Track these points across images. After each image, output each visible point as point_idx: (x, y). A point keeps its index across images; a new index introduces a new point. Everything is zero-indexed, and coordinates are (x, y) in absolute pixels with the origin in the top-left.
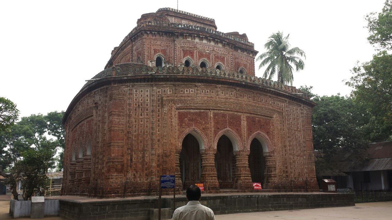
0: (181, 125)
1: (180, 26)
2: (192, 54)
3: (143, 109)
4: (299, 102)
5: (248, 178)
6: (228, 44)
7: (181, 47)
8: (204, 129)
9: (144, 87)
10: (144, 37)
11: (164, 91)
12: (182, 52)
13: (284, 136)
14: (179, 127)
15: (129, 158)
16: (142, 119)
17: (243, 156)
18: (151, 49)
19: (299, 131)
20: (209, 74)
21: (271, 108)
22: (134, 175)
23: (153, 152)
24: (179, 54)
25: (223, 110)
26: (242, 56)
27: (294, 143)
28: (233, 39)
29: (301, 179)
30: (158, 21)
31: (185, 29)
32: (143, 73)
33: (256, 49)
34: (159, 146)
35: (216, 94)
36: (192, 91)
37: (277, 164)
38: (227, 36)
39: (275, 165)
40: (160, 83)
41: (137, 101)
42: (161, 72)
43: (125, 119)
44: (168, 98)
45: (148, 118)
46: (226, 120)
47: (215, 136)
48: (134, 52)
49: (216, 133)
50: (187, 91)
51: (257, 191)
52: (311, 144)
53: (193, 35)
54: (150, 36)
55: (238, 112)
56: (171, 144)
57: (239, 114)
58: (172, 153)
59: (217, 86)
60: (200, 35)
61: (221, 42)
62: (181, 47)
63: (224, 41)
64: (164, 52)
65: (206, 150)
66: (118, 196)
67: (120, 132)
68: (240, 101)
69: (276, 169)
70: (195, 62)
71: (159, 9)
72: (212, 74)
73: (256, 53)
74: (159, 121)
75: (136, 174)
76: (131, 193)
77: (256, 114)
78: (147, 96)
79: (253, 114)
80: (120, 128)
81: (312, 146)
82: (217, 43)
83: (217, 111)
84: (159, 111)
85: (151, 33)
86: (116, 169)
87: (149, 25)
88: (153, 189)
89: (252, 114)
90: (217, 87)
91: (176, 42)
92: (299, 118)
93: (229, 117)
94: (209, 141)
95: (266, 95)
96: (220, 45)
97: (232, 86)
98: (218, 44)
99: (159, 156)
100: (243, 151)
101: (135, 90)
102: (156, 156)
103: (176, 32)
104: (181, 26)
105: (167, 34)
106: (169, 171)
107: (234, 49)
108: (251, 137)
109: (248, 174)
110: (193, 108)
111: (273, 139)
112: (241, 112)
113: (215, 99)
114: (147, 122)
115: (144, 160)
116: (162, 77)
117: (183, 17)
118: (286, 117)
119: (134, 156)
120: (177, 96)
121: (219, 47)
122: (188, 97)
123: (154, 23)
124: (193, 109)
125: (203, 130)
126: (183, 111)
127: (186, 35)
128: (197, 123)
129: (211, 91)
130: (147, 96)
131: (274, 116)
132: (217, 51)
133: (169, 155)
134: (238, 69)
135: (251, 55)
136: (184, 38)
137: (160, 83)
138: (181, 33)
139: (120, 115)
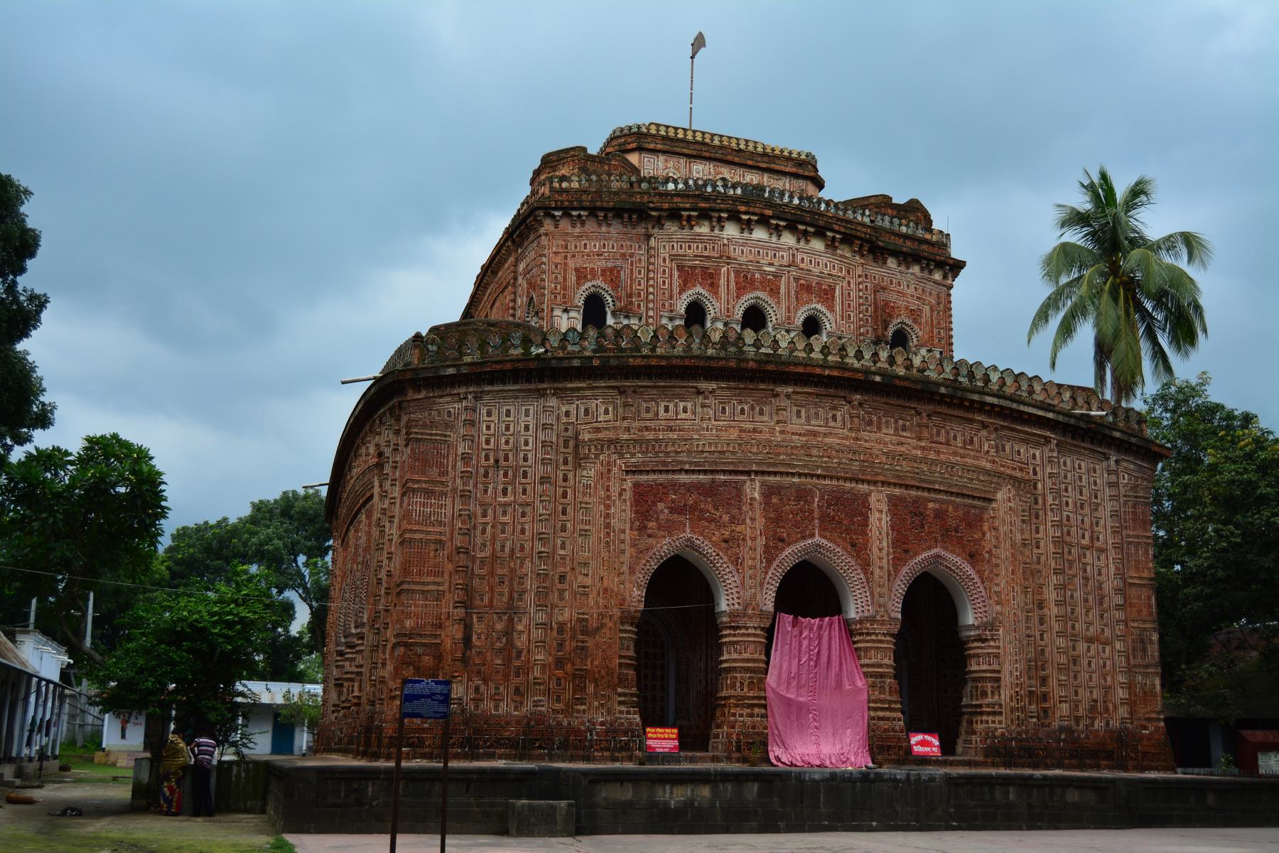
0: (642, 528)
1: (671, 186)
2: (710, 279)
3: (510, 473)
4: (1100, 446)
5: (888, 714)
6: (847, 240)
7: (673, 258)
8: (726, 541)
9: (517, 397)
10: (542, 231)
11: (587, 411)
12: (676, 273)
14: (636, 533)
15: (460, 635)
16: (506, 505)
17: (873, 637)
18: (565, 270)
19: (1101, 550)
20: (752, 349)
21: (988, 466)
22: (477, 689)
23: (541, 617)
25: (800, 475)
26: (904, 282)
28: (867, 220)
29: (1098, 724)
30: (595, 172)
31: (688, 196)
32: (512, 351)
33: (956, 253)
35: (776, 419)
37: (1007, 668)
38: (845, 210)
39: (999, 672)
40: (570, 385)
41: (491, 446)
42: (576, 348)
44: (593, 436)
45: (528, 504)
46: (811, 512)
48: (520, 279)
49: (770, 555)
50: (667, 410)
51: (924, 760)
52: (1149, 598)
53: (716, 215)
54: (565, 224)
55: (857, 481)
56: (606, 590)
57: (864, 488)
58: (606, 620)
59: (779, 389)
61: (820, 234)
62: (673, 258)
64: (612, 275)
65: (733, 615)
66: (423, 756)
67: (433, 546)
69: (999, 687)
70: (724, 310)
71: (614, 132)
72: (763, 350)
73: (956, 267)
74: (564, 513)
75: (482, 688)
76: (462, 746)
77: (929, 490)
78: (527, 428)
79: (918, 488)
80: (432, 537)
81: (1150, 606)
82: (805, 236)
83: (778, 478)
84: (565, 479)
85: (567, 214)
87: (562, 191)
89: (912, 487)
91: (652, 242)
92: (1099, 501)
93: (822, 498)
94: (743, 583)
95: (971, 421)
96: (817, 245)
98: (807, 241)
99: (561, 629)
100: (872, 620)
101: (484, 411)
102: (551, 628)
103: (653, 209)
104: (675, 182)
105: (622, 217)
106: (595, 681)
107: (871, 257)
108: (905, 570)
109: (890, 702)
110: (687, 467)
111: (992, 580)
112: (869, 482)
113: (768, 436)
114: (524, 515)
115: (510, 643)
116: (576, 363)
117: (694, 153)
118: (1050, 499)
119: (478, 627)
120: (628, 429)
121: (813, 253)
122: (670, 429)
123: (580, 181)
124: (687, 472)
125: (724, 545)
126: (651, 477)
128: (700, 519)
130: (527, 428)
131: (999, 496)
132: (801, 266)
133: (597, 630)
134: (886, 328)
135: (937, 276)
136: (682, 228)
137: (570, 385)
139: (433, 492)
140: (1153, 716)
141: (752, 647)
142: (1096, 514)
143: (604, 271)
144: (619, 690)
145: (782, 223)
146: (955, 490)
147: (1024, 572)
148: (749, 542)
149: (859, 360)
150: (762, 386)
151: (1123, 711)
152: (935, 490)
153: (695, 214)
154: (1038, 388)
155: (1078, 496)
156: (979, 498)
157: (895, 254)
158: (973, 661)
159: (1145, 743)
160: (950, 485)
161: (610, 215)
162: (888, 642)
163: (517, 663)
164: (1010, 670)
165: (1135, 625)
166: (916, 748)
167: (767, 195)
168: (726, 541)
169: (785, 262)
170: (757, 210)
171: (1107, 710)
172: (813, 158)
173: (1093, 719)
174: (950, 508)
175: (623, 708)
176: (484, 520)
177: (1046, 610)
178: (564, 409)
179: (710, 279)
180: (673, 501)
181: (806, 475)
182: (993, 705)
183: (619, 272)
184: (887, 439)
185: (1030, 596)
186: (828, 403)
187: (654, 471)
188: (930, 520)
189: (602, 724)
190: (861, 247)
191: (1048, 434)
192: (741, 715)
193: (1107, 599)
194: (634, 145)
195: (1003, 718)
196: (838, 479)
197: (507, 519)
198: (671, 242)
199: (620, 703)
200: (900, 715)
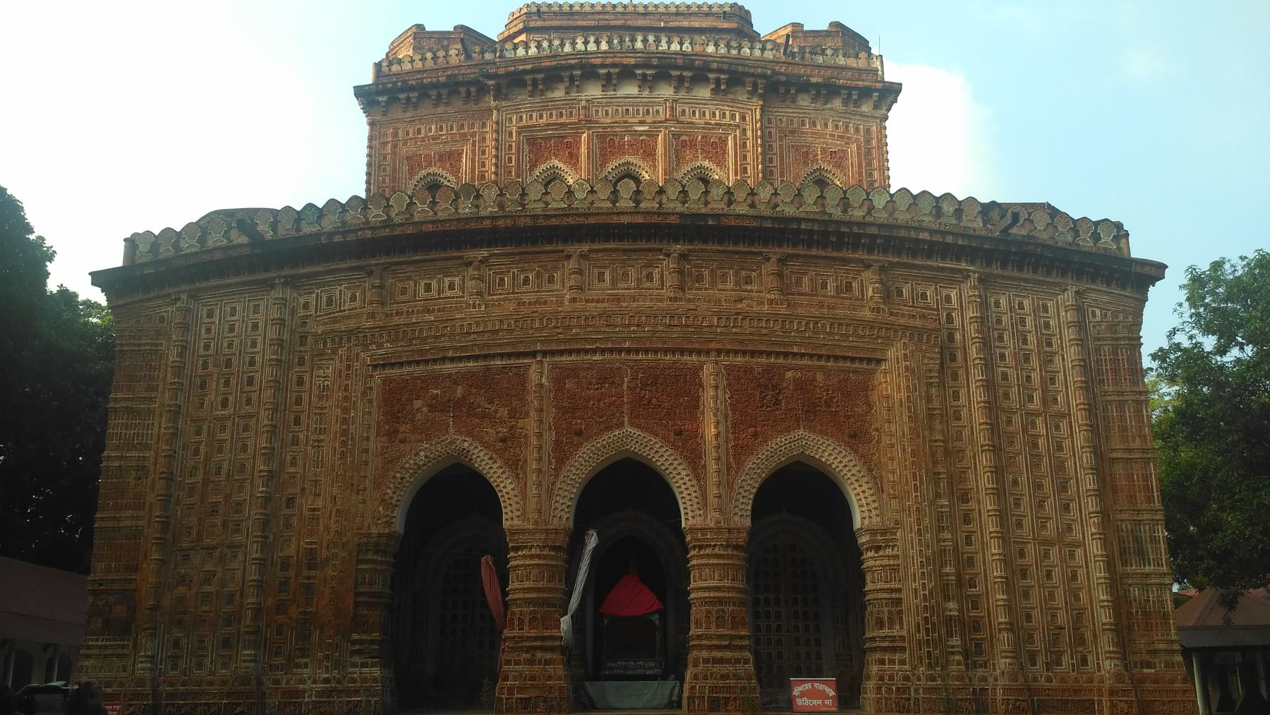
0: (393, 434)
1: (521, 52)
5: (728, 654)
12: (526, 147)
13: (958, 444)
14: (385, 439)
17: (708, 551)
22: (177, 644)
24: (510, 160)
25: (603, 351)
27: (1023, 479)
30: (430, 50)
33: (888, 78)
35: (568, 285)
36: (452, 287)
39: (899, 590)
40: (302, 271)
41: (211, 352)
43: (156, 425)
44: (329, 327)
45: (251, 417)
47: (557, 471)
50: (428, 288)
52: (1146, 478)
53: (568, 74)
55: (682, 354)
60: (596, 66)
62: (521, 130)
63: (713, 71)
68: (689, 300)
69: (900, 612)
73: (892, 92)
74: (297, 421)
77: (786, 355)
78: (255, 327)
79: (769, 354)
81: (1149, 489)
83: (573, 357)
84: (300, 382)
85: (393, 100)
88: (238, 705)
89: (761, 353)
90: (568, 257)
95: (846, 261)
96: (704, 92)
97: (648, 240)
98: (689, 90)
101: (205, 312)
109: (732, 637)
110: (450, 354)
112: (699, 352)
117: (592, 23)
118: (973, 352)
120: (372, 316)
123: (412, 61)
124: (452, 359)
126: (406, 369)
127: (535, 83)
130: (255, 327)
131: (890, 354)
132: (682, 119)
135: (866, 108)
137: (302, 271)
138: (509, 74)
140: (1161, 646)
141: (535, 571)
142: (1051, 368)
143: (441, 156)
144: (355, 637)
145: (649, 72)
147: (933, 455)
148: (534, 441)
150: (548, 248)
151: (1106, 643)
152: (795, 354)
153: (540, 76)
154: (948, 208)
156: (861, 360)
158: (868, 578)
159: (1148, 685)
161: (444, 92)
162: (729, 557)
163: (229, 608)
164: (914, 589)
165: (1125, 516)
166: (799, 702)
167: (639, 45)
168: (503, 440)
169: (662, 117)
170: (617, 60)
171: (1081, 640)
172: (741, 8)
173: (1059, 654)
174: (820, 377)
175: (357, 659)
176: (197, 439)
177: (973, 505)
178: (302, 301)
181: (611, 351)
182: (893, 639)
184: (722, 296)
185: (943, 485)
187: (410, 363)
189: (327, 681)
190: (755, 86)
191: (964, 265)
192: (517, 663)
193: (1073, 482)
194: (521, 26)
195: (907, 655)
196: (656, 351)
197: (226, 435)
199: (353, 653)
200: (748, 655)
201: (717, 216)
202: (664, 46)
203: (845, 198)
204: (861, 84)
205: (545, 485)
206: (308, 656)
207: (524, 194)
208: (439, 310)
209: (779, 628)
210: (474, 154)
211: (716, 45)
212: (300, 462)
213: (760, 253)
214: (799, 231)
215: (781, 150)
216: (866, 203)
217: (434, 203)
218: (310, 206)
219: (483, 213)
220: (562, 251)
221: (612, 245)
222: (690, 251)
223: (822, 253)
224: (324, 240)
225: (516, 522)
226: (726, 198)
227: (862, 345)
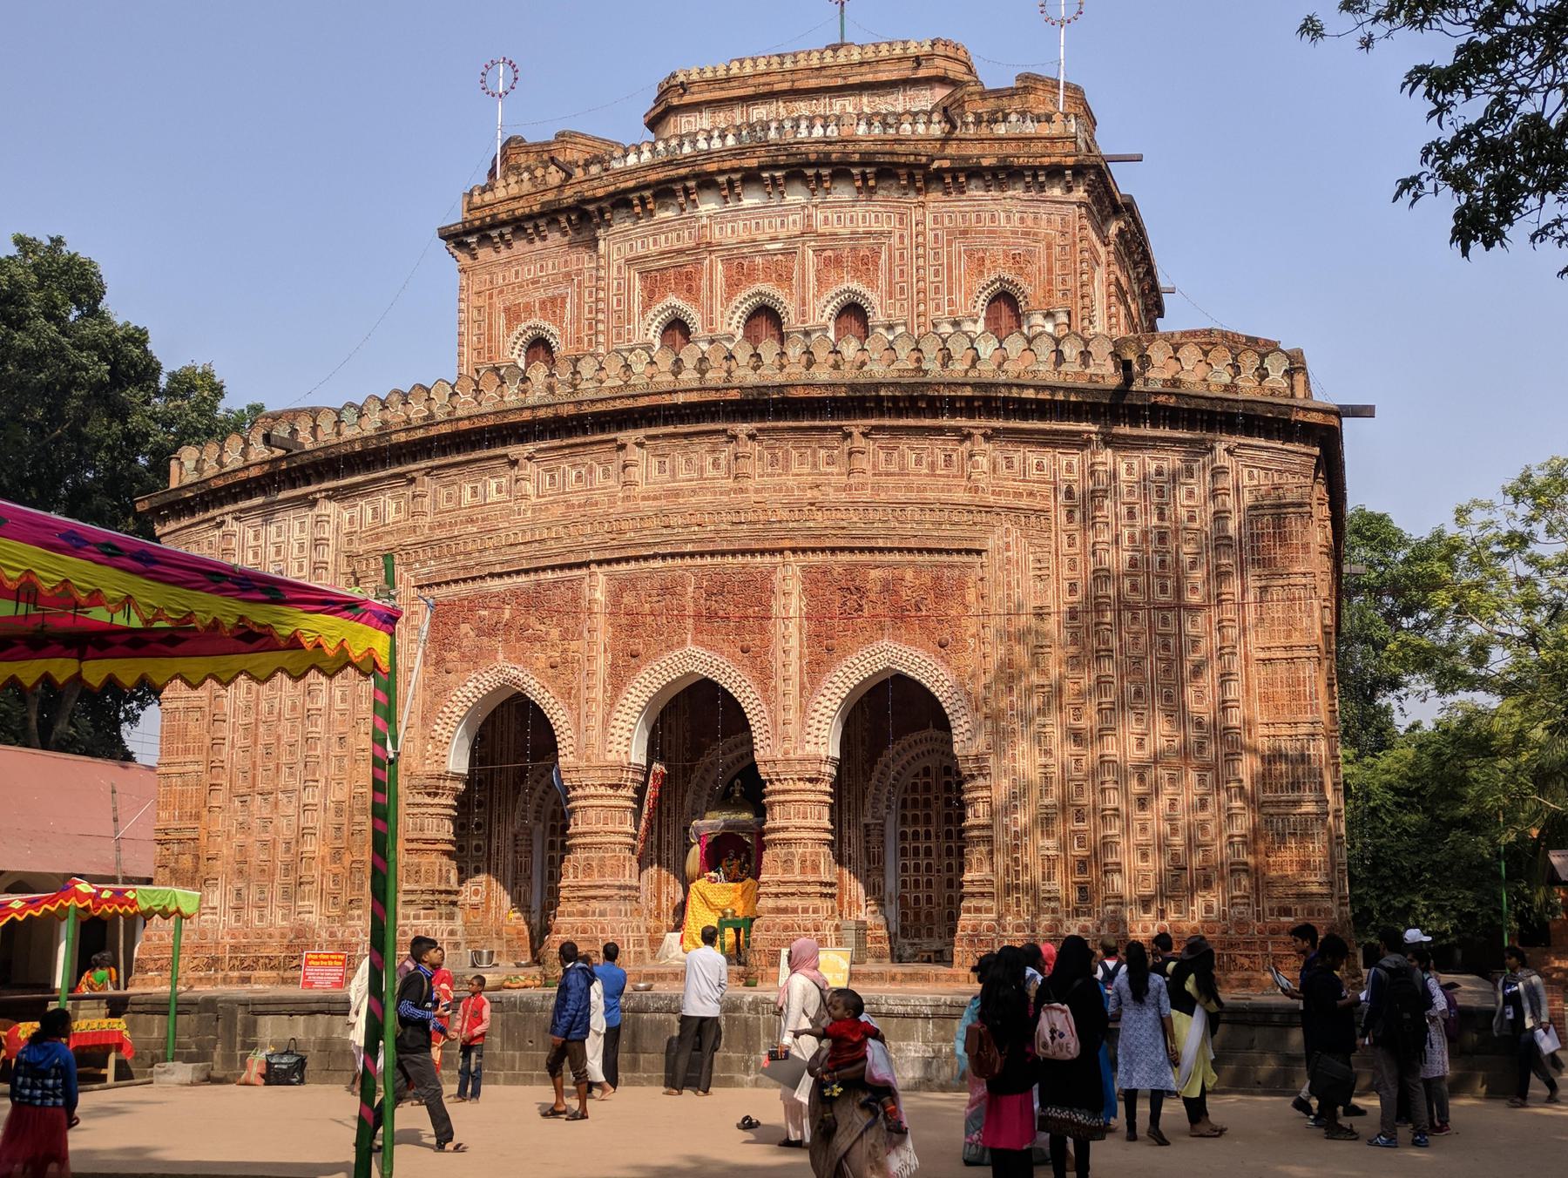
0: (440, 661)
1: (632, 159)
2: (688, 283)
7: (630, 262)
14: (432, 669)
18: (490, 314)
25: (664, 557)
30: (528, 169)
34: (341, 768)
36: (499, 491)
53: (678, 187)
54: (485, 253)
55: (753, 552)
59: (622, 436)
60: (712, 173)
61: (841, 171)
63: (855, 165)
64: (553, 305)
68: (757, 491)
75: (244, 892)
77: (871, 550)
79: (851, 550)
85: (485, 239)
86: (173, 872)
89: (842, 549)
90: (622, 447)
97: (713, 420)
99: (339, 812)
101: (251, 533)
110: (498, 569)
112: (772, 552)
117: (750, 91)
121: (840, 205)
124: (500, 575)
125: (550, 671)
128: (518, 640)
129: (599, 470)
130: (301, 546)
135: (1056, 192)
138: (610, 195)
143: (543, 303)
145: (778, 174)
146: (912, 544)
149: (755, 369)
152: (881, 550)
153: (647, 193)
155: (1155, 521)
157: (975, 173)
160: (903, 538)
161: (542, 223)
167: (772, 134)
170: (735, 163)
174: (909, 575)
179: (688, 283)
180: (482, 619)
181: (673, 556)
183: (564, 300)
184: (791, 481)
186: (702, 446)
187: (456, 581)
188: (873, 596)
190: (911, 177)
196: (723, 553)
198: (624, 241)
201: (781, 386)
202: (803, 133)
203: (945, 348)
204: (1046, 161)
205: (599, 715)
206: (359, 908)
207: (576, 373)
208: (483, 520)
209: (929, 866)
210: (579, 294)
211: (869, 124)
212: (350, 700)
213: (840, 428)
214: (879, 399)
215: (949, 257)
216: (971, 352)
217: (478, 391)
218: (352, 405)
219: (531, 401)
220: (615, 440)
221: (670, 429)
222: (759, 430)
223: (911, 422)
224: (358, 448)
225: (570, 758)
226: (804, 358)
227: (958, 533)
